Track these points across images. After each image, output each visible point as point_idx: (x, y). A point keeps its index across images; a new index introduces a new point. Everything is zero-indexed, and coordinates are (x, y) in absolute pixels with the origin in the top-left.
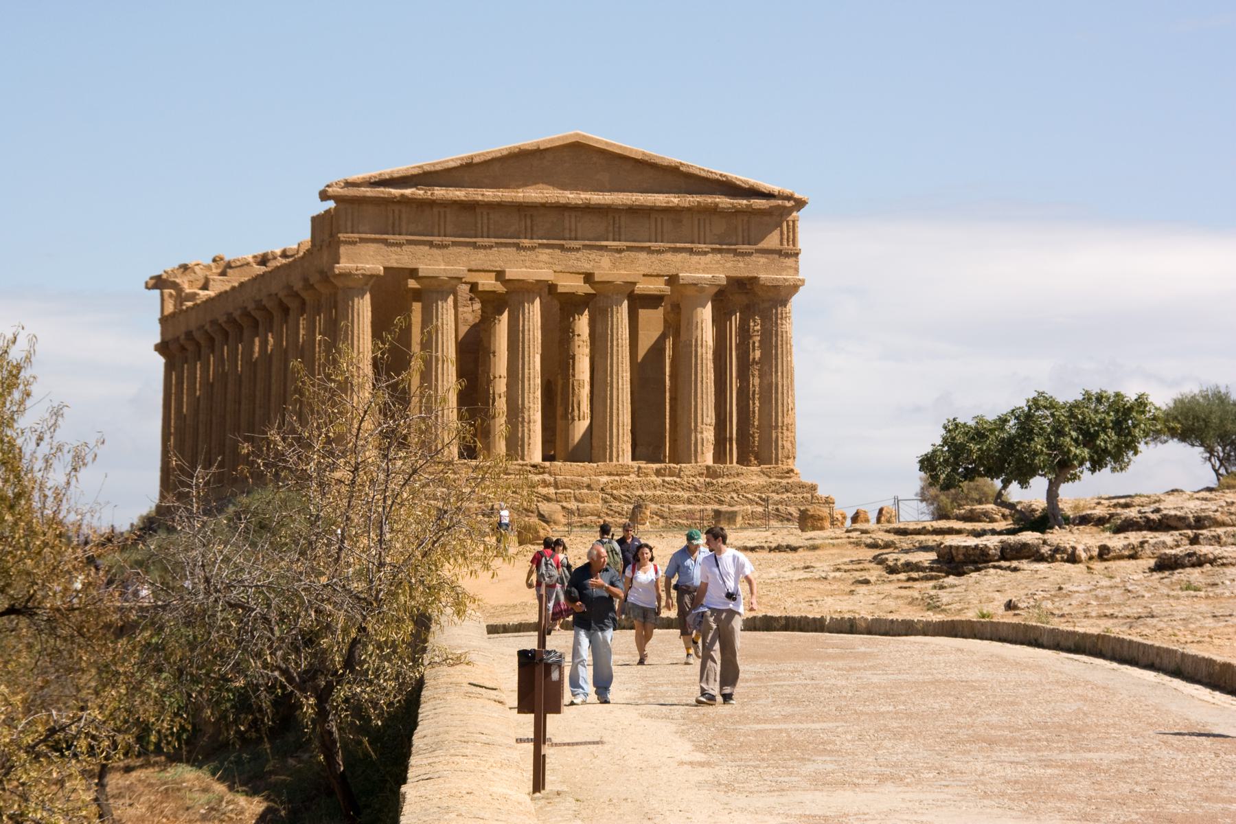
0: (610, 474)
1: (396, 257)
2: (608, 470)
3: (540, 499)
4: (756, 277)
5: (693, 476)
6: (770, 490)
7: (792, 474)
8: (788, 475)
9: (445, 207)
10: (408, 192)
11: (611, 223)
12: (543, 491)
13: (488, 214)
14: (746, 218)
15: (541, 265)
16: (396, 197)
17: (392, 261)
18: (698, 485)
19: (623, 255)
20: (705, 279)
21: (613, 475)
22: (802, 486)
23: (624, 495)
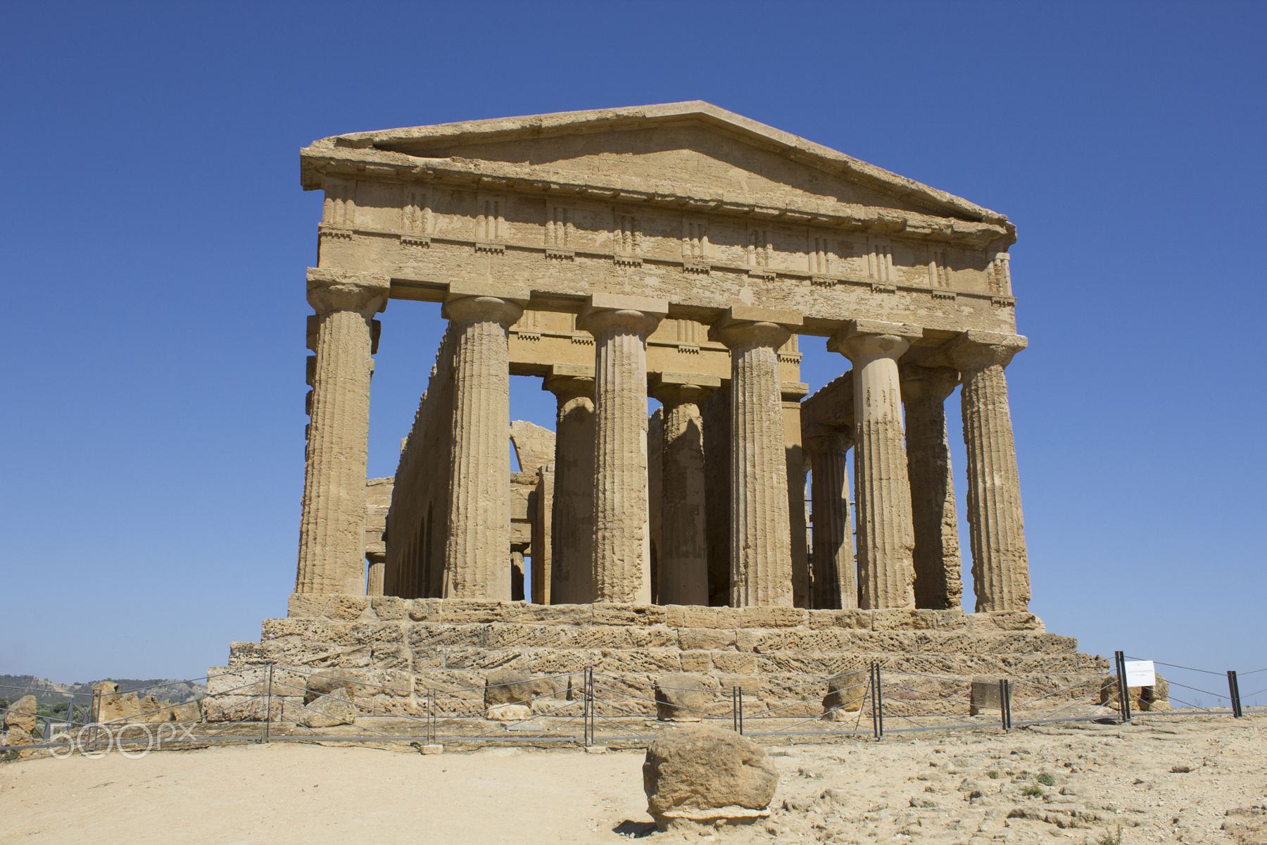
0: (763, 626)
1: (415, 264)
2: (762, 618)
3: (653, 667)
4: (958, 334)
5: (892, 628)
6: (1012, 647)
7: (1033, 625)
8: (1027, 625)
9: (498, 196)
10: (435, 161)
11: (753, 237)
12: (658, 652)
13: (565, 211)
14: (940, 251)
15: (648, 291)
16: (417, 167)
17: (406, 270)
18: (906, 642)
19: (770, 285)
20: (893, 328)
21: (772, 626)
22: (1055, 641)
23: (794, 660)
